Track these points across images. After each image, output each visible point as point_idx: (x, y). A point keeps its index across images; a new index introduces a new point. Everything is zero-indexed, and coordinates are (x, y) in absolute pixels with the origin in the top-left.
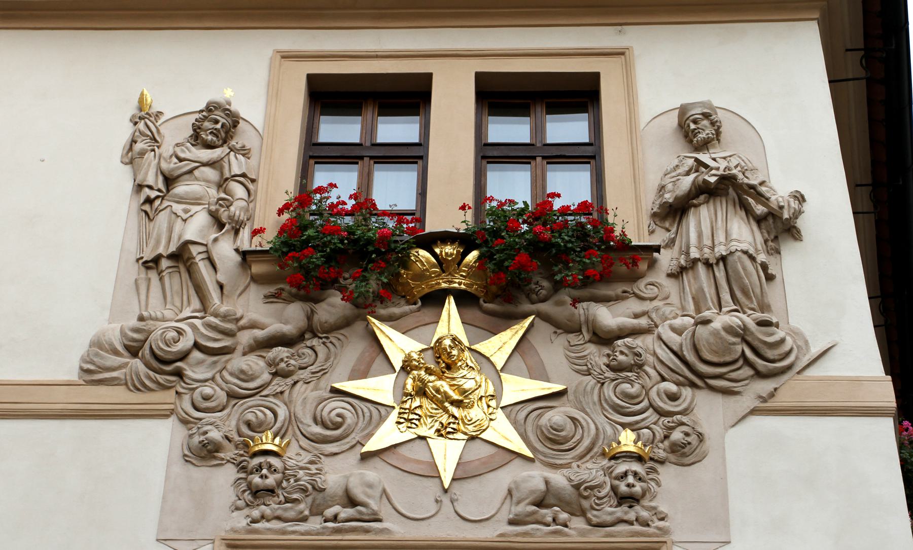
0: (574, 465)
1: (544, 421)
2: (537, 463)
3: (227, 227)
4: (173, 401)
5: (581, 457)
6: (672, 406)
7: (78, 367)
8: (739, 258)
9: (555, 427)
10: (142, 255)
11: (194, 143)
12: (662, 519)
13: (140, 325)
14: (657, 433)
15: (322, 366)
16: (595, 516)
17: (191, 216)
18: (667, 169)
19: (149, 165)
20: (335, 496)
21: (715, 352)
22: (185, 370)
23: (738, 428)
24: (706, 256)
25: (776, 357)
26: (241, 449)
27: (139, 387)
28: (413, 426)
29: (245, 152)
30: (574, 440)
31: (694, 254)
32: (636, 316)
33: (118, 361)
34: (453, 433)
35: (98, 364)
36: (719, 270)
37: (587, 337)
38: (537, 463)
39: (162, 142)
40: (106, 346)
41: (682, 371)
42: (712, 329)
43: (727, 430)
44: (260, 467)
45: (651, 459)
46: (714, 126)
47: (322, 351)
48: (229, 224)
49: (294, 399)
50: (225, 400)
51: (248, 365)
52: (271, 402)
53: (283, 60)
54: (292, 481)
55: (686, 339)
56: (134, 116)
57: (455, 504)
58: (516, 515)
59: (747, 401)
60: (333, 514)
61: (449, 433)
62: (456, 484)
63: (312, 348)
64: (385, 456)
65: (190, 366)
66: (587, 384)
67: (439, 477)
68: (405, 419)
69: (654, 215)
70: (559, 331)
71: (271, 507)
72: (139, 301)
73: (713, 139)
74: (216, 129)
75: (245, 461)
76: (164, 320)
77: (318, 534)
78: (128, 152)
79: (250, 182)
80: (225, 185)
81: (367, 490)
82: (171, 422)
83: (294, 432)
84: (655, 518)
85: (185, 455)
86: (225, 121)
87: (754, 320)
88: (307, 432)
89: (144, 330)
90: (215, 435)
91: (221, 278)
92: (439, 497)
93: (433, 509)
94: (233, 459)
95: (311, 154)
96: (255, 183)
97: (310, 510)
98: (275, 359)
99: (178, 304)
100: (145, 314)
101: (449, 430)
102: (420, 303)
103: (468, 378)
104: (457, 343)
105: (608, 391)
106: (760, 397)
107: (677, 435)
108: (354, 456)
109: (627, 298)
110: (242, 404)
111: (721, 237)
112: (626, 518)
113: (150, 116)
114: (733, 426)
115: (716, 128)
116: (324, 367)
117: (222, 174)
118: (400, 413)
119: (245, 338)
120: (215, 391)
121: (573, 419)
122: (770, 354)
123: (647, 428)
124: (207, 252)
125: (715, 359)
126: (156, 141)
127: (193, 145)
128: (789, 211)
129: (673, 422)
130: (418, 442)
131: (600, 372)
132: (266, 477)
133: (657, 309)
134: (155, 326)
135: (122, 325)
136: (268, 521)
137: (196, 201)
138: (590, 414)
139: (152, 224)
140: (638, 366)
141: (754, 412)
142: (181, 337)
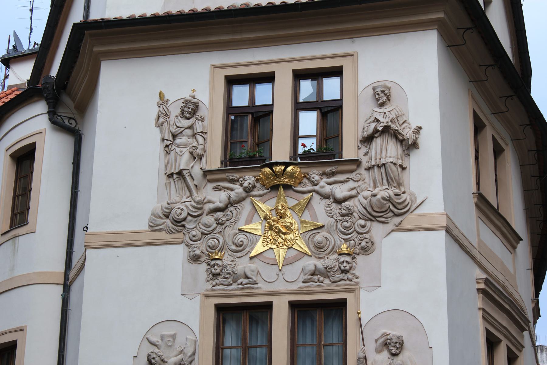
0: (326, 257)
1: (315, 239)
4: (182, 237)
5: (329, 254)
9: (319, 242)
10: (166, 172)
11: (182, 116)
12: (357, 278)
13: (167, 206)
14: (356, 242)
15: (235, 219)
16: (332, 279)
17: (183, 154)
18: (366, 119)
19: (166, 129)
21: (379, 208)
23: (385, 238)
24: (378, 163)
25: (402, 208)
27: (170, 232)
28: (268, 243)
29: (202, 120)
30: (326, 247)
31: (373, 163)
32: (352, 189)
33: (163, 221)
34: (282, 246)
35: (155, 224)
36: (383, 169)
37: (332, 200)
39: (170, 116)
40: (157, 215)
41: (367, 215)
44: (214, 265)
45: (354, 253)
48: (197, 157)
49: (225, 234)
50: (201, 236)
52: (217, 236)
53: (215, 69)
54: (225, 270)
55: (368, 203)
56: (158, 103)
57: (283, 275)
58: (304, 280)
59: (390, 227)
62: (283, 266)
63: (231, 211)
64: (258, 257)
65: (187, 223)
66: (331, 223)
67: (278, 265)
68: (265, 241)
69: (361, 141)
70: (322, 198)
71: (219, 280)
73: (386, 102)
74: (189, 111)
75: (209, 262)
76: (177, 203)
77: (236, 290)
78: (157, 122)
79: (204, 134)
82: (183, 245)
83: (226, 248)
84: (354, 278)
85: (188, 260)
86: (193, 107)
87: (394, 193)
88: (231, 248)
89: (169, 208)
90: (198, 252)
91: (196, 183)
92: (278, 273)
93: (276, 277)
96: (207, 134)
97: (233, 281)
98: (217, 218)
99: (181, 194)
100: (169, 202)
101: (281, 245)
102: (270, 189)
103: (288, 221)
104: (283, 208)
105: (339, 225)
106: (396, 225)
107: (363, 244)
108: (247, 258)
109: (349, 181)
110: (207, 238)
111: (384, 155)
112: (344, 278)
113: (164, 103)
114: (385, 237)
115: (387, 96)
116: (235, 220)
117: (194, 132)
118: (263, 239)
119: (208, 207)
120: (197, 233)
121: (326, 238)
122: (399, 207)
123: (353, 240)
125: (378, 210)
126: (168, 116)
127: (181, 117)
128: (411, 140)
129: (362, 238)
130: (271, 250)
131: (336, 216)
132: (216, 269)
133: (359, 186)
134: (173, 206)
135: (162, 205)
136: (218, 285)
137: (184, 146)
138: (333, 235)
139: (169, 156)
140: (350, 214)
141: (393, 231)
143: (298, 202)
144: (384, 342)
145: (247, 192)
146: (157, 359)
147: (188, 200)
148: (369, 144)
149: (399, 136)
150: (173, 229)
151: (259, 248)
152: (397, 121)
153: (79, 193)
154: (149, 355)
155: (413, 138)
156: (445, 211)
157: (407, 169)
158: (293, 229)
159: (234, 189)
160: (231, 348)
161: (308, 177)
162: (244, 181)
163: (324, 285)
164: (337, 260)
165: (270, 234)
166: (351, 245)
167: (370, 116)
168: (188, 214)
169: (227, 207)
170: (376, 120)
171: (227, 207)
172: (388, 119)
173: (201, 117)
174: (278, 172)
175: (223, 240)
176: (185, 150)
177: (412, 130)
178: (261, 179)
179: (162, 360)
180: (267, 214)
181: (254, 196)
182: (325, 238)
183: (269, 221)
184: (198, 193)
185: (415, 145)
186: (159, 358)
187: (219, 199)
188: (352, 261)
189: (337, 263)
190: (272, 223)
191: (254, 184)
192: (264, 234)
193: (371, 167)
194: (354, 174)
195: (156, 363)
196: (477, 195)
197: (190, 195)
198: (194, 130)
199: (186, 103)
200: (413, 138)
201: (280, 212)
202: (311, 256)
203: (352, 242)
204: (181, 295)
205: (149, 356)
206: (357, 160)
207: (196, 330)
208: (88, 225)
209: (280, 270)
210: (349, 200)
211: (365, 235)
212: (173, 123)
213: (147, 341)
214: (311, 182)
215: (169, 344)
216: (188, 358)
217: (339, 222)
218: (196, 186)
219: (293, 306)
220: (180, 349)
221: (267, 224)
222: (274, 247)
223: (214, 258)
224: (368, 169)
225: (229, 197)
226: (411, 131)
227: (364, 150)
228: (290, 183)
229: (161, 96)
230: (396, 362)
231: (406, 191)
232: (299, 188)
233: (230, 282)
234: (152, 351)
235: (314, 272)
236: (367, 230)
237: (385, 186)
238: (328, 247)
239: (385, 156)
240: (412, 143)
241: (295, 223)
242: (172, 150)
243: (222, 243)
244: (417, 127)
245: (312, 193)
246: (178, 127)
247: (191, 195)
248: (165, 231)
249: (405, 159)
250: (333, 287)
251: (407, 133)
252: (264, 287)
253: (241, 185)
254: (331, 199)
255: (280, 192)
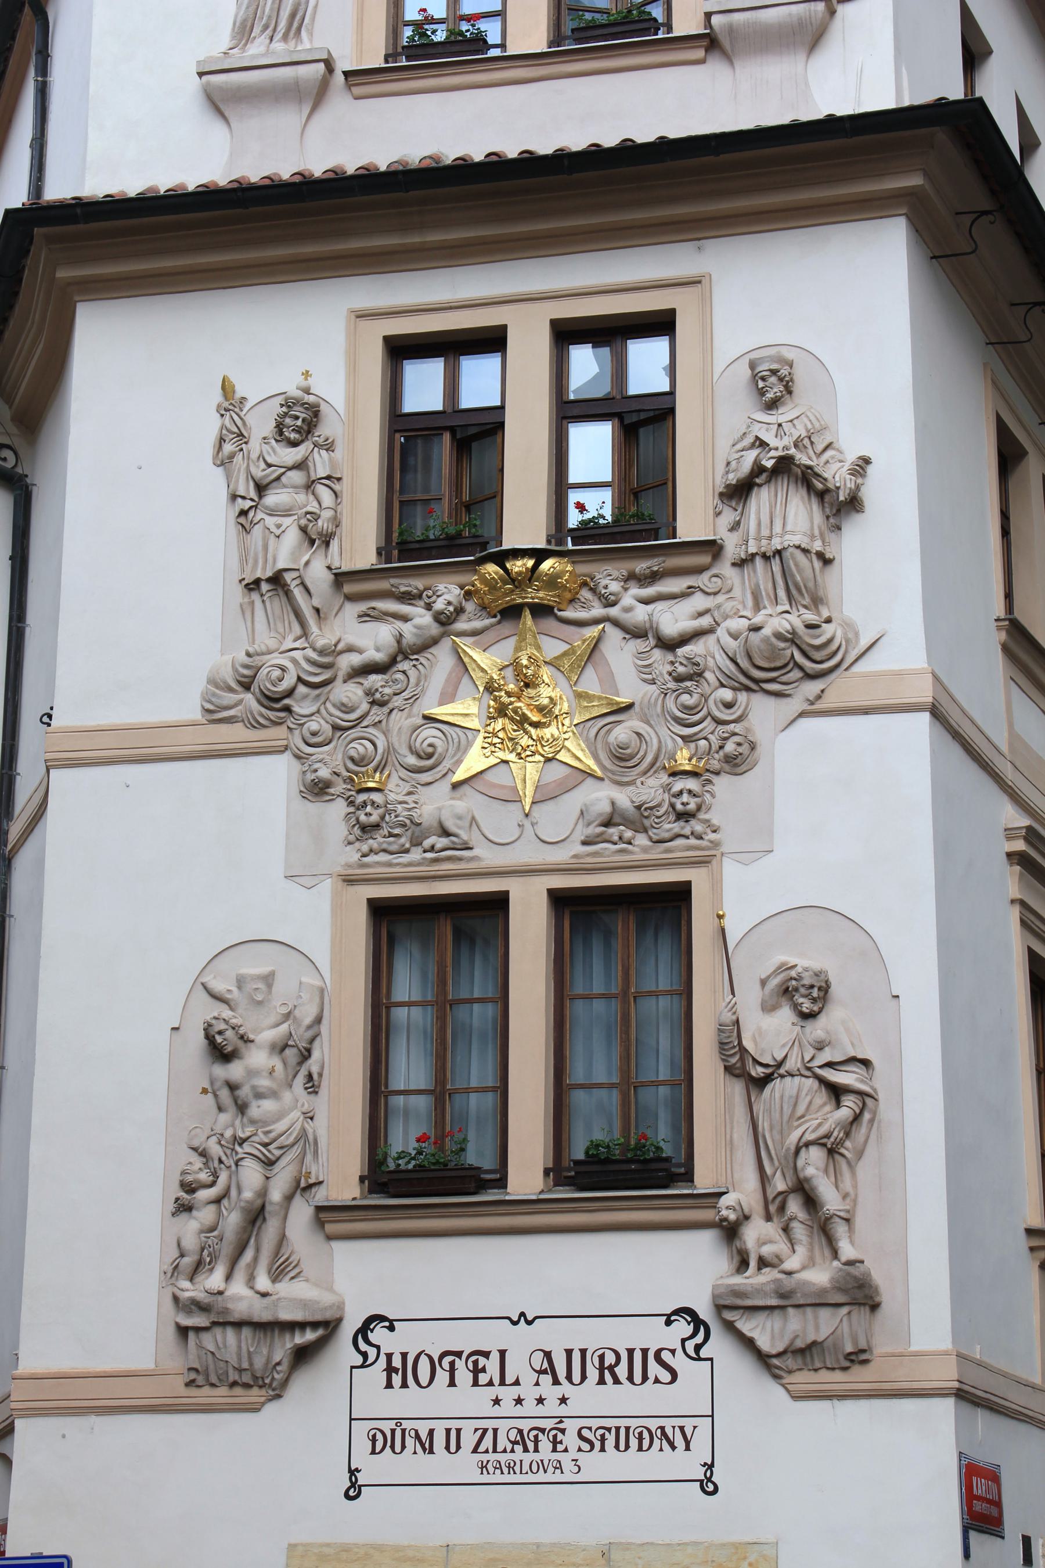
0: (638, 782)
1: (611, 738)
2: (607, 781)
3: (317, 541)
4: (285, 737)
5: (645, 773)
6: (727, 714)
7: (199, 708)
8: (792, 554)
9: (621, 745)
10: (244, 576)
11: (279, 438)
12: (714, 831)
13: (247, 660)
14: (712, 744)
15: (414, 691)
16: (655, 834)
17: (283, 532)
20: (431, 828)
21: (768, 659)
22: (293, 706)
24: (763, 549)
25: (824, 658)
26: (348, 783)
28: (497, 749)
29: (329, 447)
30: (639, 756)
31: (752, 549)
32: (701, 614)
34: (532, 755)
35: (218, 704)
37: (652, 641)
38: (607, 781)
39: (249, 437)
40: (221, 684)
41: (737, 677)
42: (762, 636)
43: (777, 735)
44: (364, 804)
45: (708, 770)
46: (782, 381)
47: (413, 674)
48: (319, 539)
50: (330, 734)
51: (347, 697)
53: (358, 319)
54: (393, 815)
55: (739, 647)
56: (219, 406)
57: (535, 827)
58: (587, 837)
59: (796, 704)
60: (430, 845)
61: (528, 756)
62: (534, 806)
63: (404, 672)
64: (473, 783)
65: (297, 701)
66: (651, 697)
67: (521, 801)
69: (721, 495)
70: (627, 636)
72: (246, 628)
73: (782, 396)
74: (297, 426)
75: (352, 796)
76: (270, 652)
77: (419, 864)
78: (218, 452)
79: (336, 481)
80: (312, 488)
81: (458, 822)
82: (287, 756)
83: (392, 759)
84: (708, 831)
85: (301, 791)
86: (306, 416)
87: (803, 622)
88: (404, 763)
89: (252, 666)
90: (324, 773)
91: (316, 602)
92: (521, 821)
94: (342, 793)
95: (397, 427)
96: (341, 482)
98: (370, 690)
99: (281, 630)
100: (251, 650)
102: (499, 617)
103: (545, 694)
104: (533, 661)
106: (808, 700)
107: (730, 747)
108: (445, 786)
109: (693, 593)
110: (348, 736)
111: (778, 528)
112: (682, 832)
113: (234, 406)
115: (784, 383)
116: (415, 693)
119: (347, 662)
120: (321, 725)
121: (638, 734)
122: (817, 656)
123: (705, 738)
124: (300, 576)
125: (766, 665)
126: (245, 438)
127: (277, 441)
128: (844, 492)
129: (727, 732)
130: (503, 766)
132: (370, 815)
136: (376, 854)
137: (287, 513)
139: (249, 536)
140: (697, 676)
141: (802, 714)
142: (285, 674)
143: (570, 646)
144: (781, 986)
145: (442, 624)
146: (229, 1033)
147: (297, 645)
148: (742, 501)
149: (814, 481)
150: (262, 715)
151: (474, 761)
152: (809, 443)
153: (28, 630)
154: (210, 1025)
155: (849, 485)
156: (929, 663)
157: (836, 563)
158: (557, 712)
159: (410, 617)
160: (409, 1004)
161: (592, 584)
162: (434, 597)
163: (636, 849)
164: (667, 788)
165: (500, 727)
166: (700, 752)
167: (745, 434)
168: (299, 679)
169: (393, 661)
170: (758, 443)
171: (393, 661)
172: (787, 441)
173: (327, 440)
174: (519, 573)
175: (386, 743)
176: (287, 521)
177: (847, 466)
178: (477, 591)
179: (242, 1037)
180: (492, 678)
181: (460, 634)
182: (635, 735)
183: (497, 694)
184: (323, 627)
185: (854, 503)
186: (234, 1032)
187: (375, 642)
188: (703, 791)
189: (666, 796)
190: (506, 699)
191: (461, 604)
192: (487, 725)
193: (746, 559)
194: (705, 576)
195: (226, 1045)
196: (1007, 623)
197: (303, 633)
198: (309, 473)
199: (289, 407)
200: (851, 485)
201: (525, 672)
202: (601, 779)
203: (703, 742)
204: (285, 877)
205: (210, 1028)
206: (712, 543)
207: (324, 962)
208: (52, 708)
209: (527, 815)
210: (695, 640)
211: (733, 725)
212: (257, 455)
213: (204, 991)
214: (599, 598)
215: (255, 997)
216: (305, 1031)
217: (668, 694)
218: (317, 610)
219: (559, 899)
220: (284, 1010)
221: (492, 703)
222: (512, 757)
223: (364, 786)
224: (740, 564)
225: (399, 639)
226: (846, 468)
227: (729, 516)
228: (549, 600)
229: (227, 388)
230: (811, 1033)
231: (834, 616)
232: (570, 614)
233: (403, 845)
234: (216, 1014)
235: (611, 818)
236: (739, 713)
237: (782, 604)
238: (644, 757)
239: (781, 532)
240: (846, 499)
241: (561, 698)
242: (255, 522)
243: (384, 750)
244: (860, 458)
245: (602, 625)
246: (269, 466)
247: (305, 634)
248: (243, 721)
249: (832, 537)
250: (657, 853)
251: (835, 474)
252: (486, 856)
253: (429, 607)
254: (651, 639)
255: (524, 623)
